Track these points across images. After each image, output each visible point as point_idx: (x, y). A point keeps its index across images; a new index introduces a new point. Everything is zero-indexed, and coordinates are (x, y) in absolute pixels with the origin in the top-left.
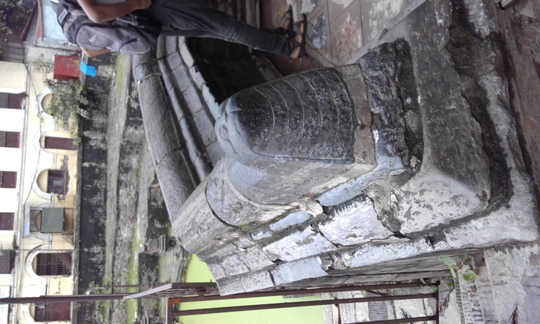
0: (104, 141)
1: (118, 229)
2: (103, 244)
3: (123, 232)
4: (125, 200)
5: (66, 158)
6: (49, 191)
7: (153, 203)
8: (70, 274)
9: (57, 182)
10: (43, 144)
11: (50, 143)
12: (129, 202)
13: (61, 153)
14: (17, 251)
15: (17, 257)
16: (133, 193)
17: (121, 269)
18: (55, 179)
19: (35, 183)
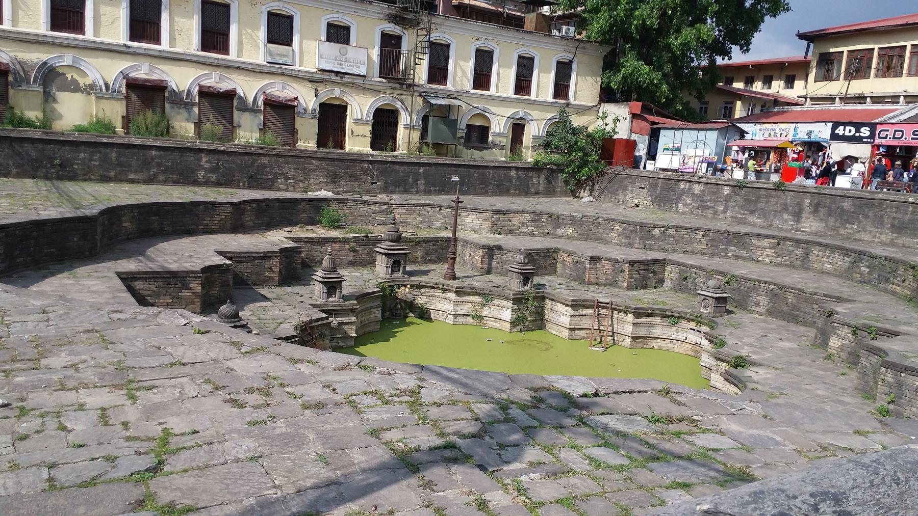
0: (537, 193)
1: (478, 211)
2: (428, 192)
3: (474, 217)
4: (516, 220)
5: (502, 147)
6: (468, 126)
7: (542, 255)
8: (373, 147)
9: (475, 135)
10: (517, 122)
11: (518, 129)
12: (514, 225)
13: (506, 141)
14: (405, 87)
15: (398, 86)
16: (524, 230)
17: (420, 215)
18: (478, 135)
19: (479, 111)
